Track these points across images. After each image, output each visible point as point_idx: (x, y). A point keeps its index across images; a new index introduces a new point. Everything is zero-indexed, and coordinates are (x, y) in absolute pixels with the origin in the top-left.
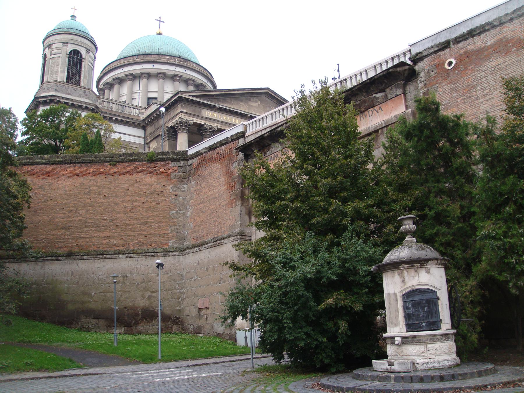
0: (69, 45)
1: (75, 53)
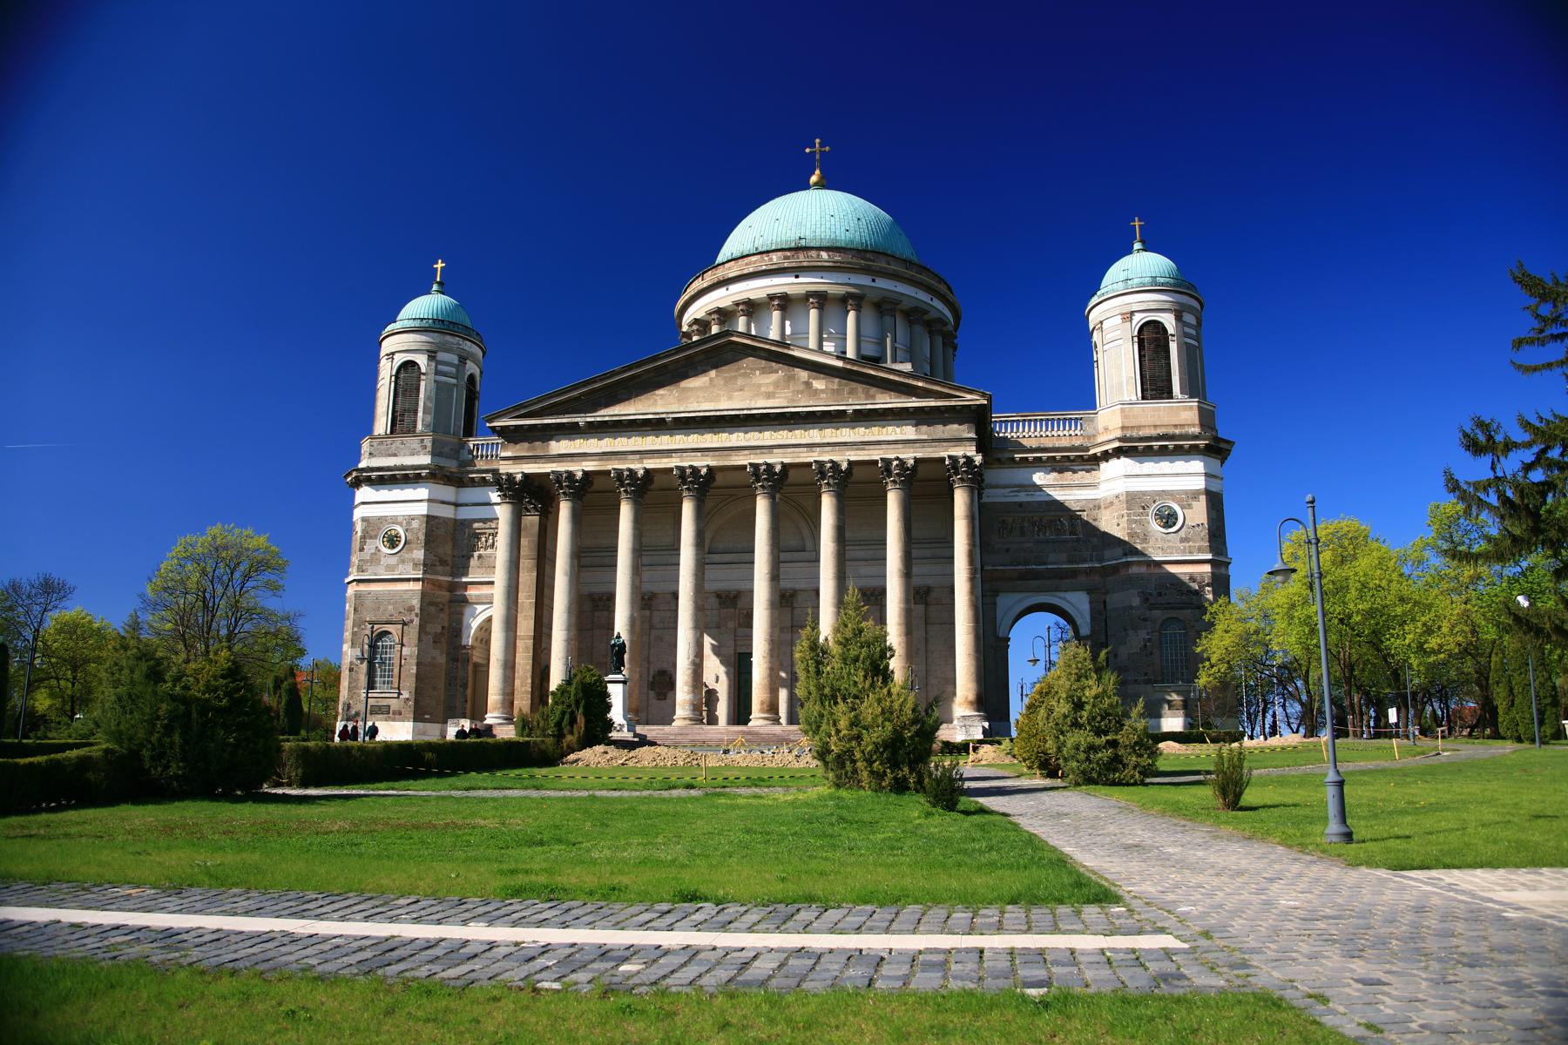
0: (396, 356)
1: (409, 366)
